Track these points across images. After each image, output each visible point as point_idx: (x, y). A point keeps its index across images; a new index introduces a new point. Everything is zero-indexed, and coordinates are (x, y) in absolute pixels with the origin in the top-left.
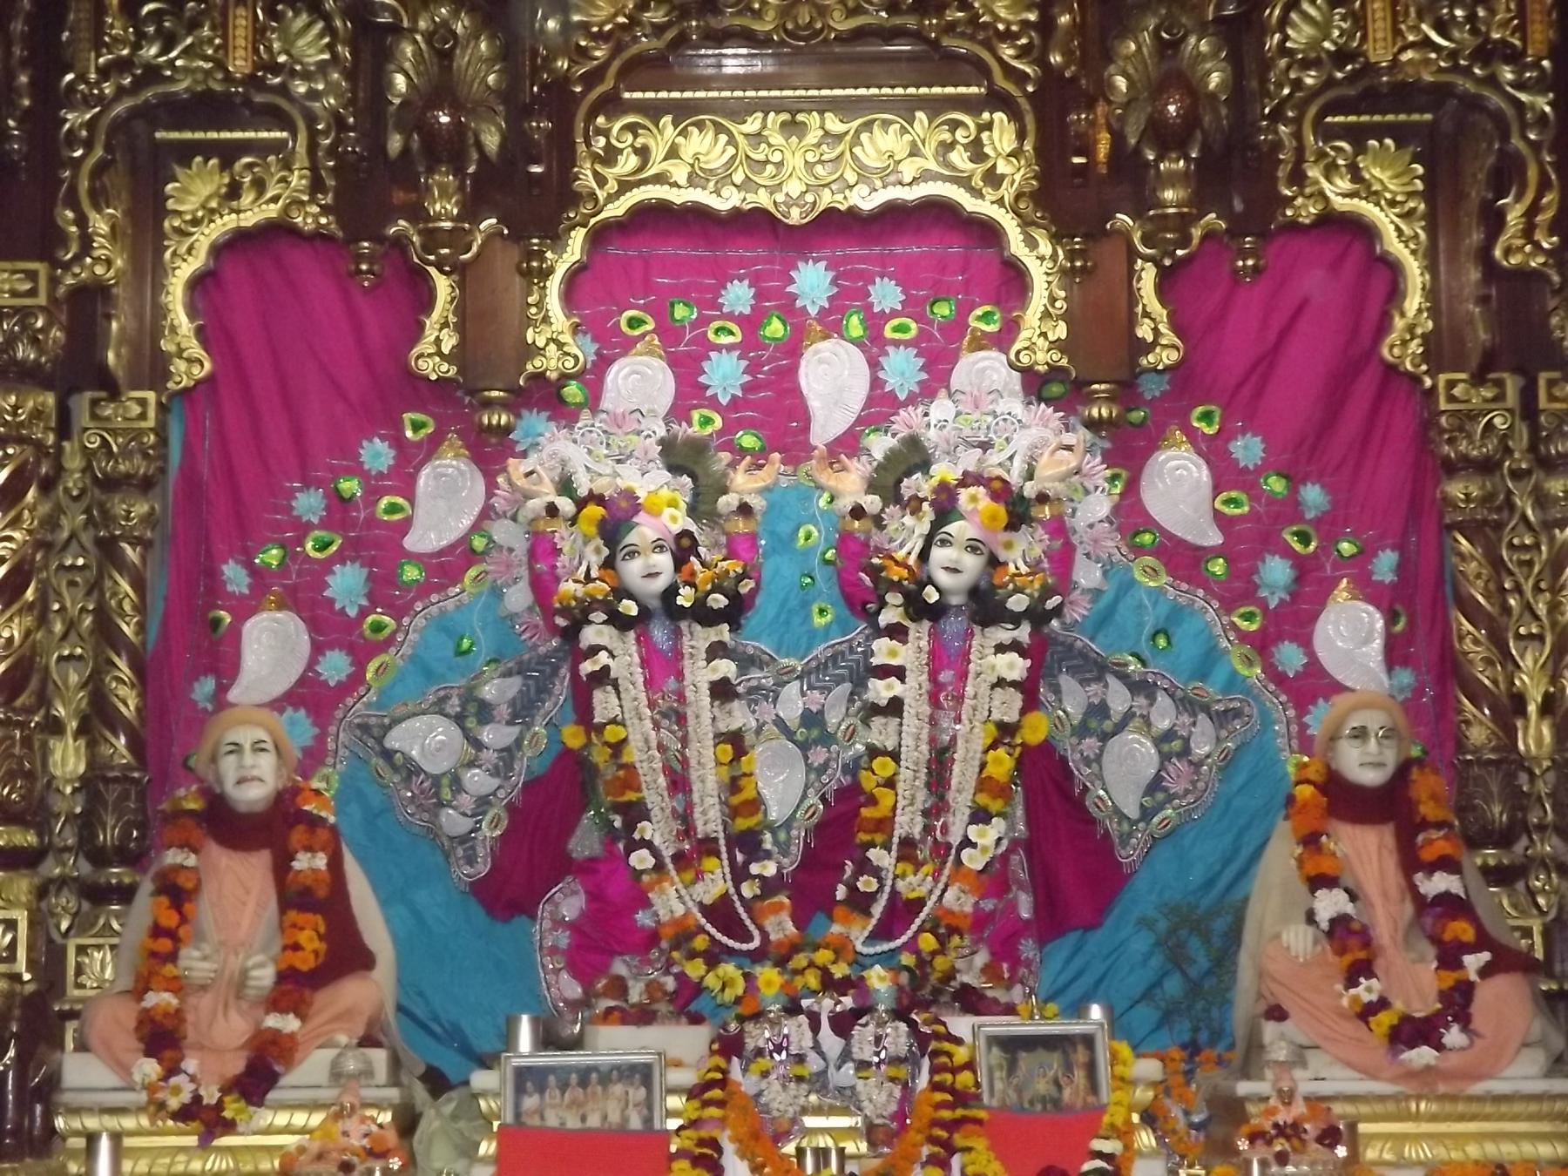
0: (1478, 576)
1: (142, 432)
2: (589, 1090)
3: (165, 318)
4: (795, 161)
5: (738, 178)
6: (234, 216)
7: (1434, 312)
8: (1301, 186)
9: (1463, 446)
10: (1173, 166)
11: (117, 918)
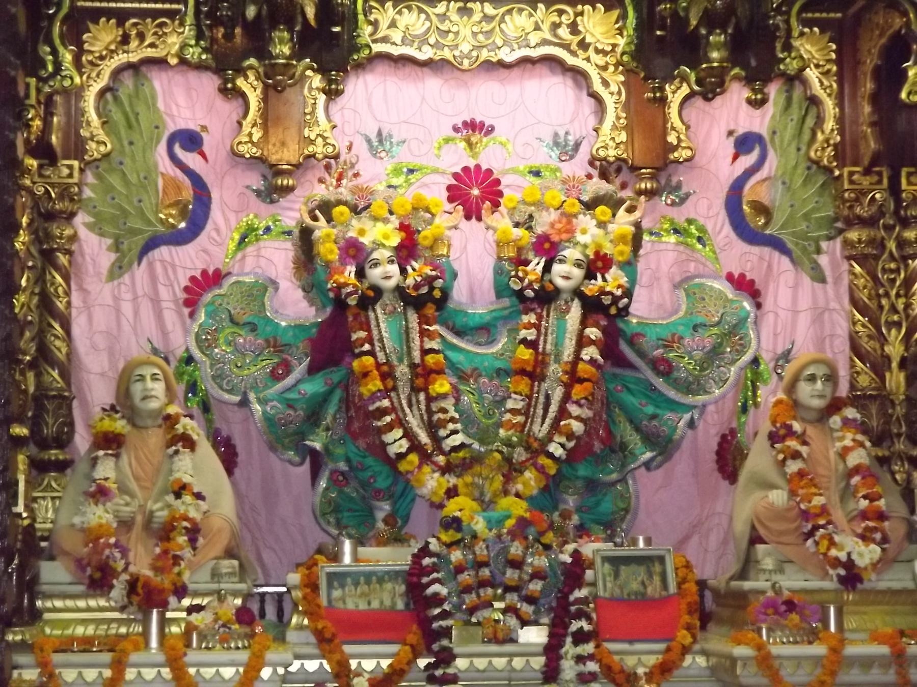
0: (865, 287)
1: (70, 185)
2: (372, 586)
3: (83, 116)
4: (466, 32)
5: (432, 41)
6: (125, 55)
7: (841, 132)
8: (790, 53)
9: (858, 210)
10: (717, 38)
11: (56, 481)
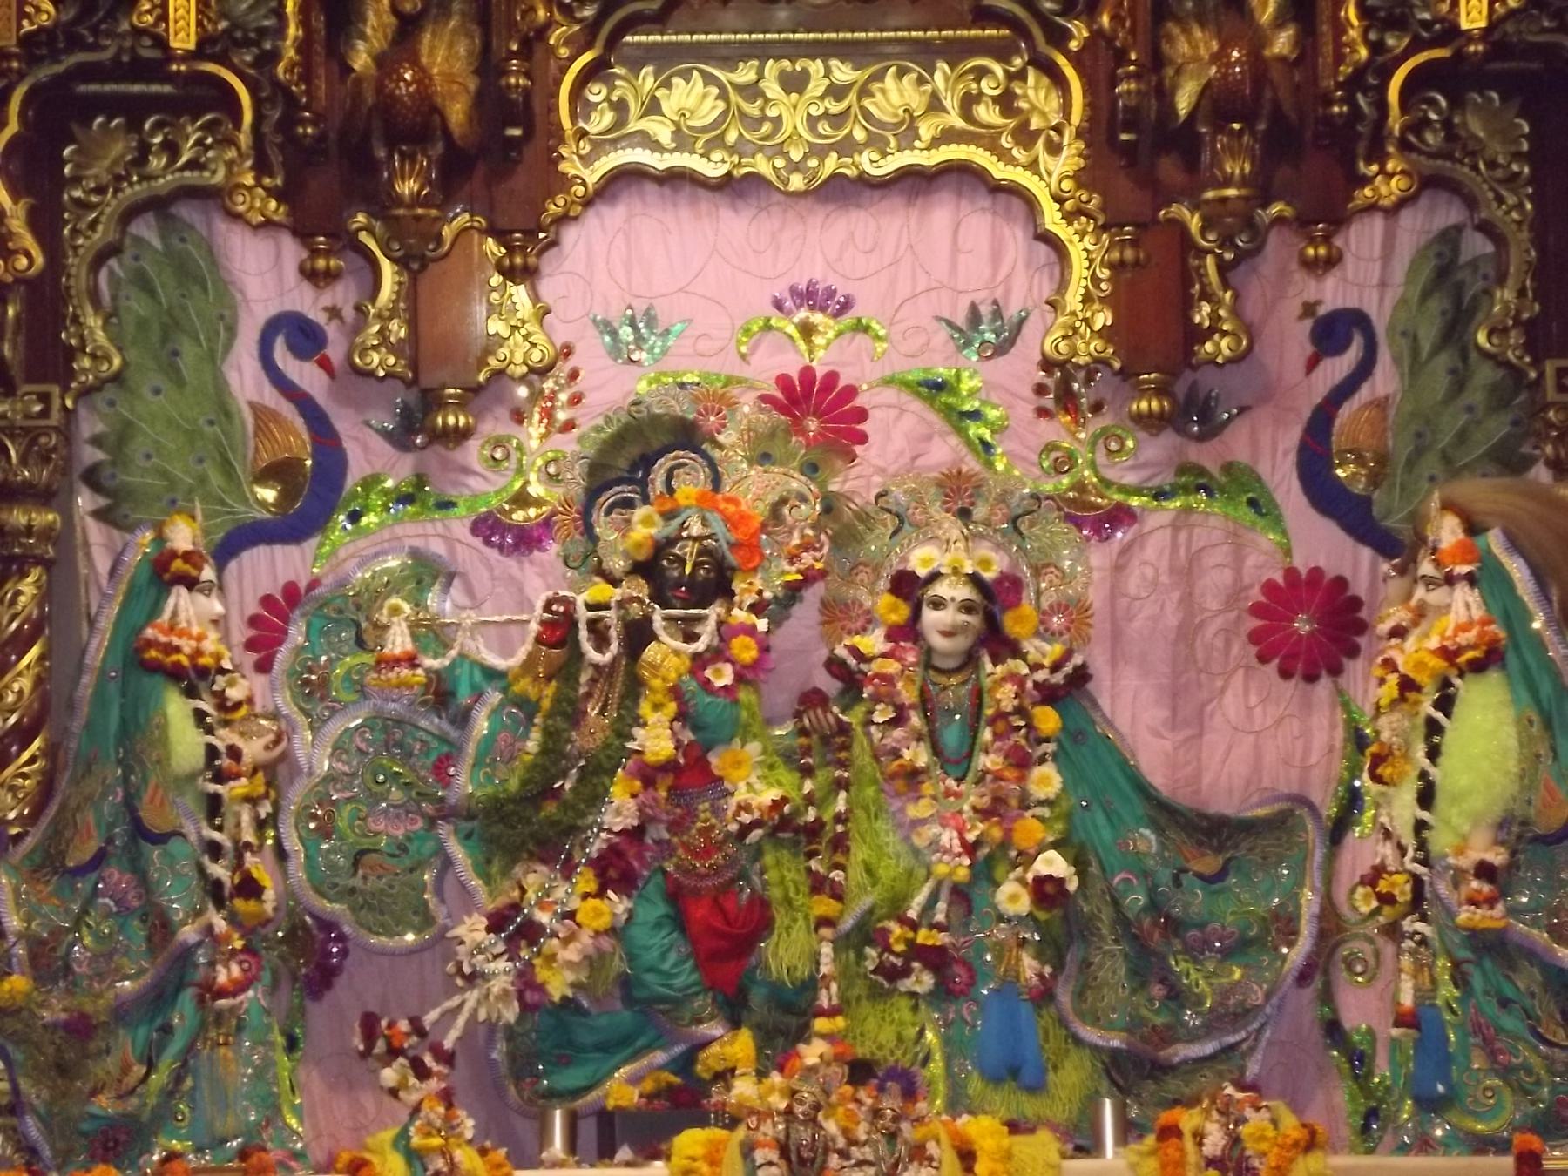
5: (731, 137)
